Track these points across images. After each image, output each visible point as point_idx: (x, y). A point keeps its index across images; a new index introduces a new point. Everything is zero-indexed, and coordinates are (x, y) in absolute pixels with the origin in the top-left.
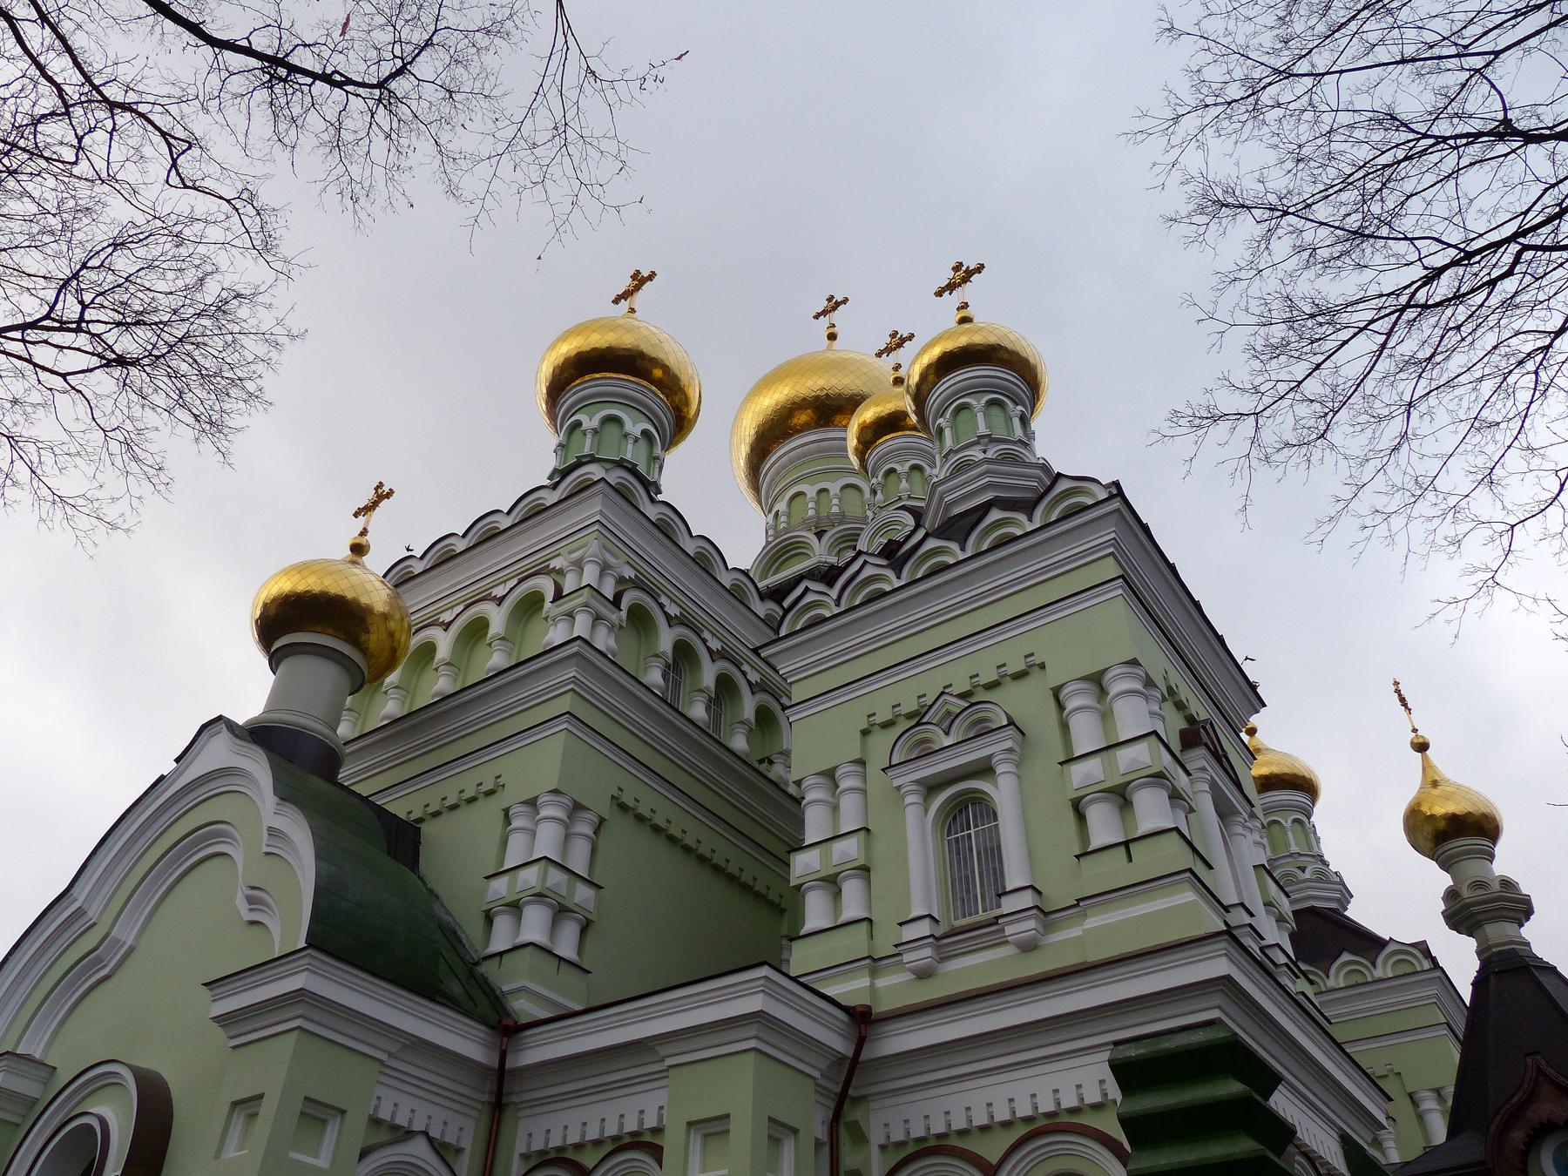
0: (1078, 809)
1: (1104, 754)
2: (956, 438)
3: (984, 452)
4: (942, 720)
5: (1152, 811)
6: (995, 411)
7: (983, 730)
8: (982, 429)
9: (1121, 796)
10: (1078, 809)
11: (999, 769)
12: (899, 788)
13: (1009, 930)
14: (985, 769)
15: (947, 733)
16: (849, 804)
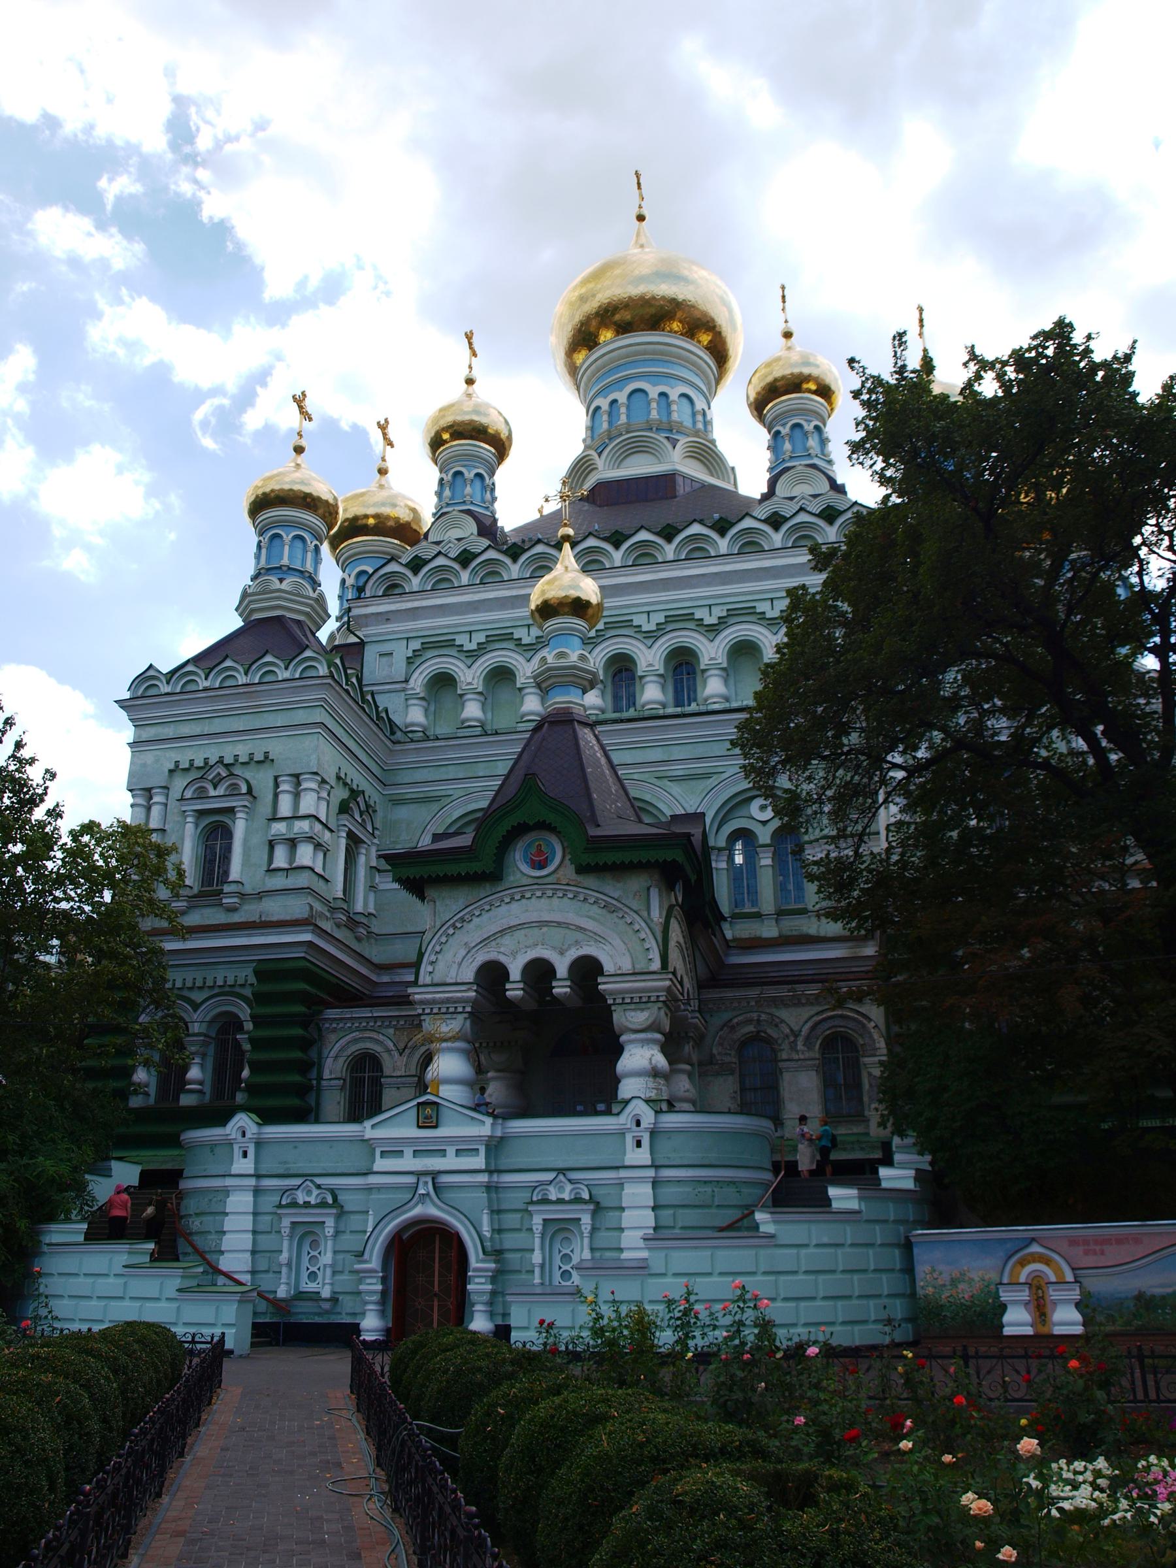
0: (271, 845)
1: (288, 820)
2: (268, 560)
4: (214, 778)
5: (305, 855)
6: (299, 544)
7: (234, 791)
9: (292, 843)
10: (271, 845)
11: (239, 815)
12: (184, 811)
13: (224, 901)
14: (231, 811)
15: (215, 788)
16: (156, 811)
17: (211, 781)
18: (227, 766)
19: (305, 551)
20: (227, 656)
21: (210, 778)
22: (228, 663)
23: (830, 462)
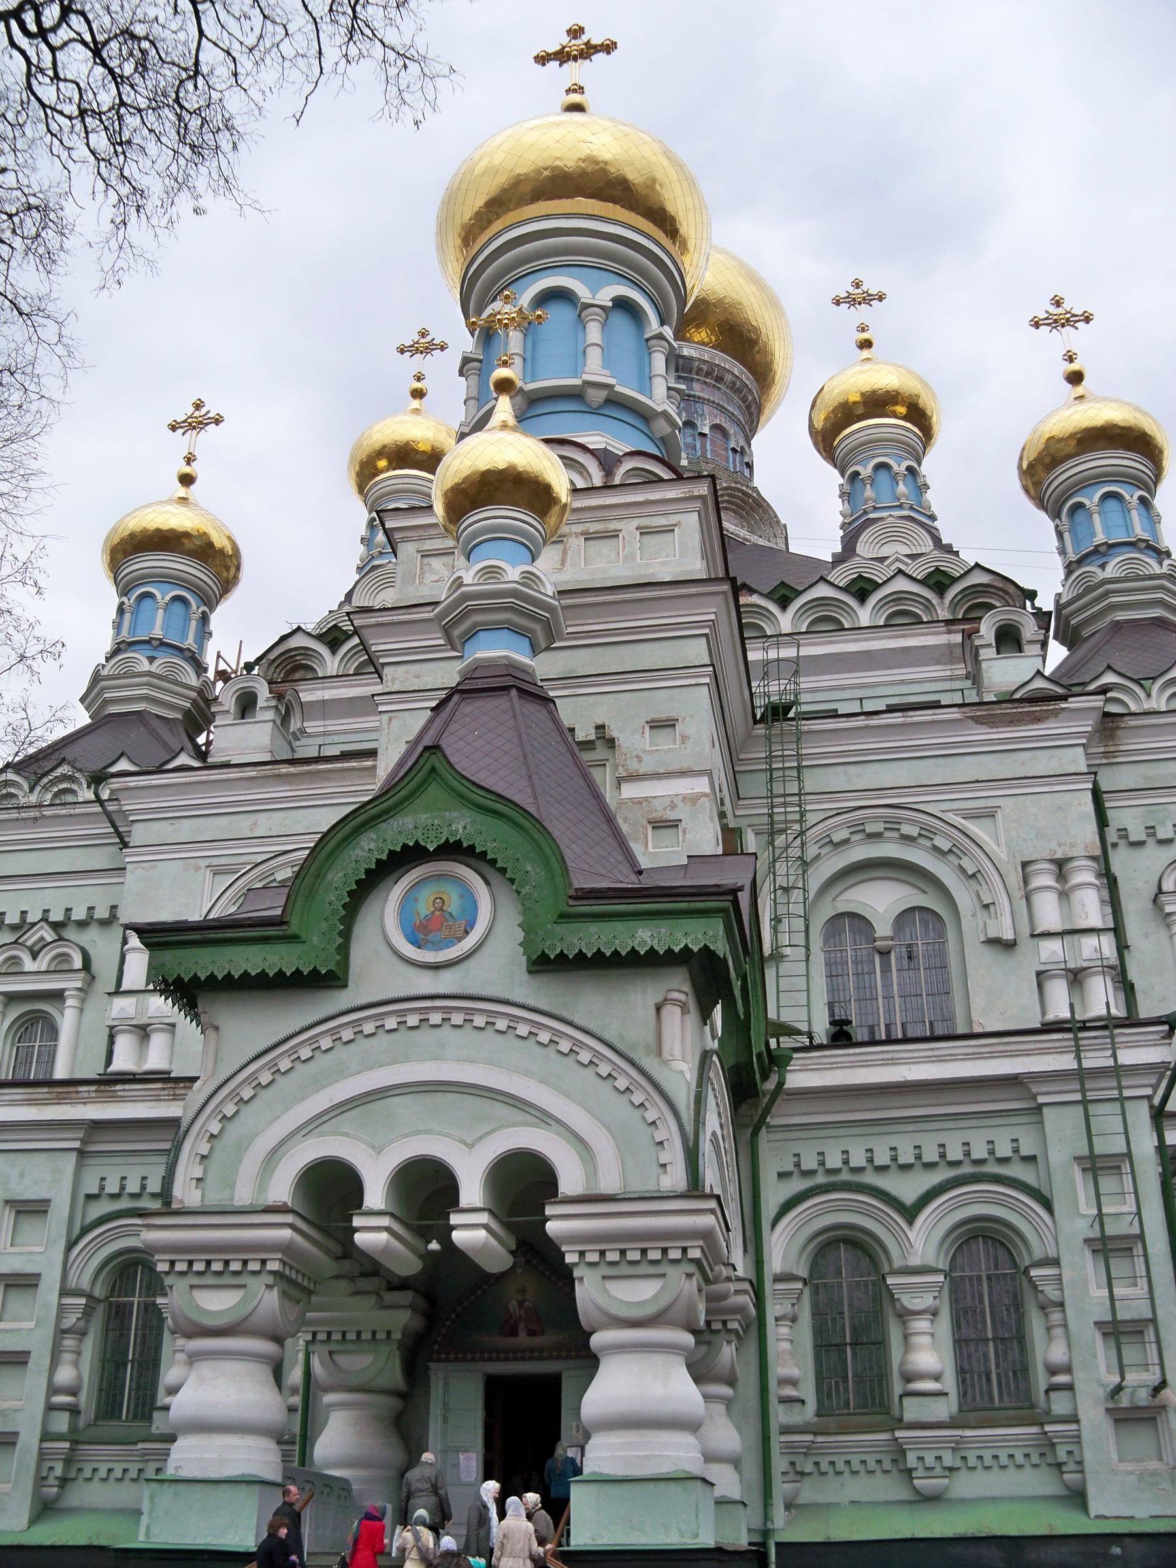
3: (151, 659)
6: (178, 608)
8: (157, 632)
11: (69, 1002)
15: (35, 956)
17: (30, 949)
18: (56, 926)
19: (187, 620)
20: (63, 761)
21: (29, 943)
22: (64, 769)
23: (933, 518)
